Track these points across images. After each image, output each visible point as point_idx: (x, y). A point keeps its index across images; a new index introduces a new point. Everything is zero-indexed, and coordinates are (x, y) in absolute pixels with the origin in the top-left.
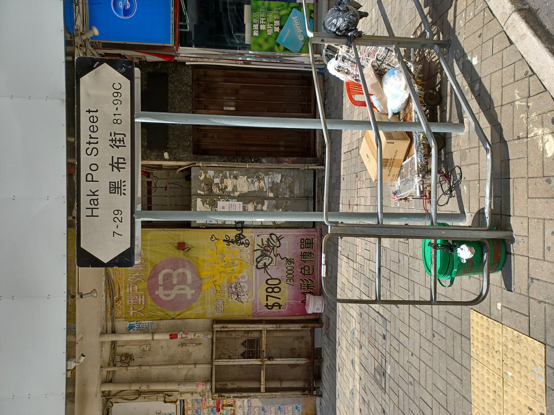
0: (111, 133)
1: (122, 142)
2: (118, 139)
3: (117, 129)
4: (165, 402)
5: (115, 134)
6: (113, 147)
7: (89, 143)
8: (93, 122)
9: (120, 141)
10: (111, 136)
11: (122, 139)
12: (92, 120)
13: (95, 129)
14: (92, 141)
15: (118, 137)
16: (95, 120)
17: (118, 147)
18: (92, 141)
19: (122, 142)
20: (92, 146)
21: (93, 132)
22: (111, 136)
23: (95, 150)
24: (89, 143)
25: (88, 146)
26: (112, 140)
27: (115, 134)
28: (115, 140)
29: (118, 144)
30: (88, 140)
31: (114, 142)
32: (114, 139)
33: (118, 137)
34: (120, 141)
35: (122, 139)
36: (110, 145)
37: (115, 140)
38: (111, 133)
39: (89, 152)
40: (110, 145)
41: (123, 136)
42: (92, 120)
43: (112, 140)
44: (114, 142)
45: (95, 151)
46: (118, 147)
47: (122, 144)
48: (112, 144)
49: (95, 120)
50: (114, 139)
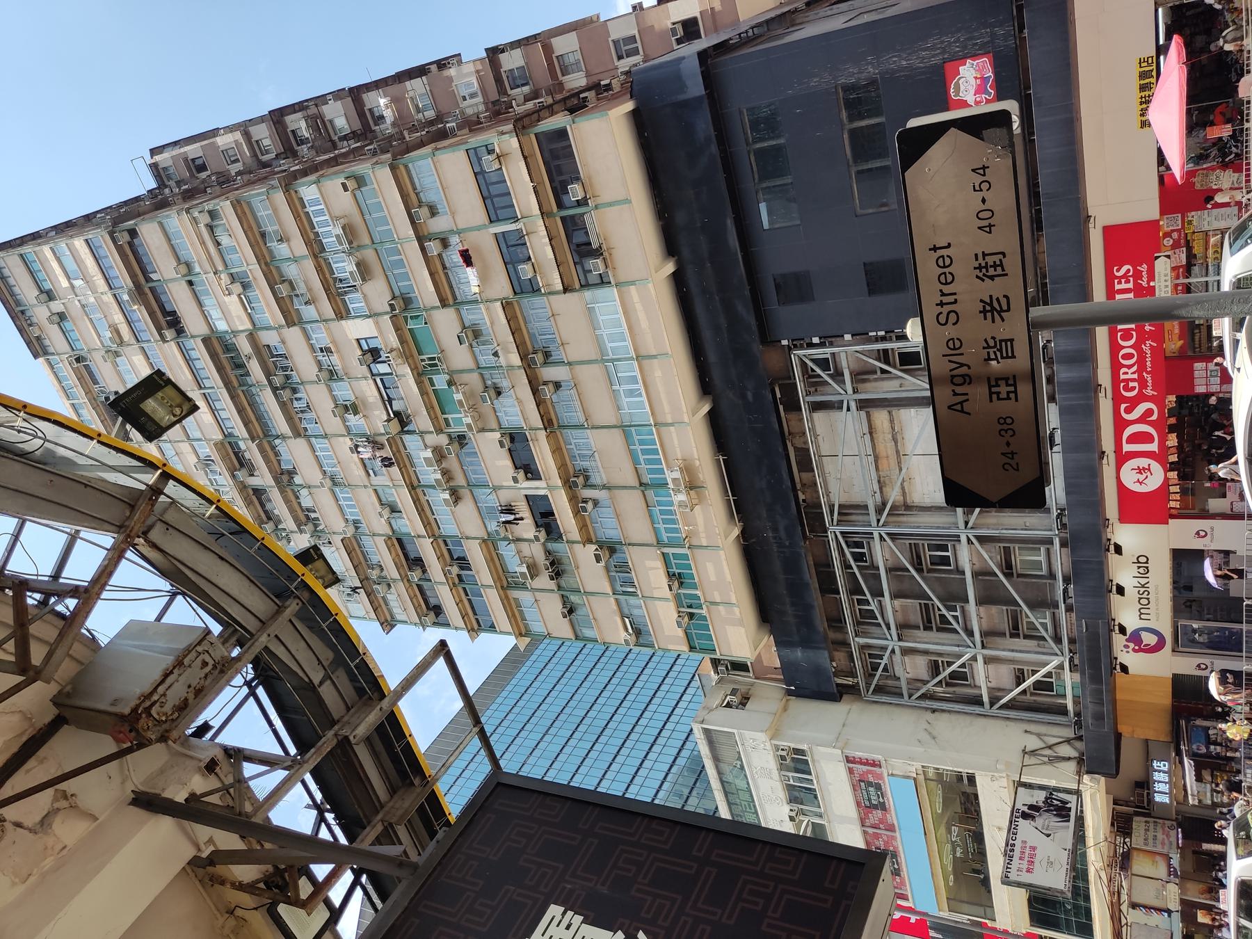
1: (999, 269)
3: (990, 243)
4: (1008, 310)
5: (984, 255)
7: (941, 304)
8: (944, 267)
12: (941, 263)
13: (950, 278)
14: (946, 299)
15: (990, 260)
16: (948, 261)
17: (992, 278)
18: (946, 299)
19: (999, 269)
20: (946, 309)
21: (946, 283)
23: (953, 316)
24: (941, 304)
25: (939, 309)
26: (980, 268)
27: (984, 255)
28: (986, 267)
29: (991, 272)
30: (938, 299)
33: (990, 260)
34: (995, 266)
37: (986, 267)
39: (942, 319)
41: (1001, 256)
42: (941, 263)
45: (953, 317)
48: (981, 275)
49: (948, 261)
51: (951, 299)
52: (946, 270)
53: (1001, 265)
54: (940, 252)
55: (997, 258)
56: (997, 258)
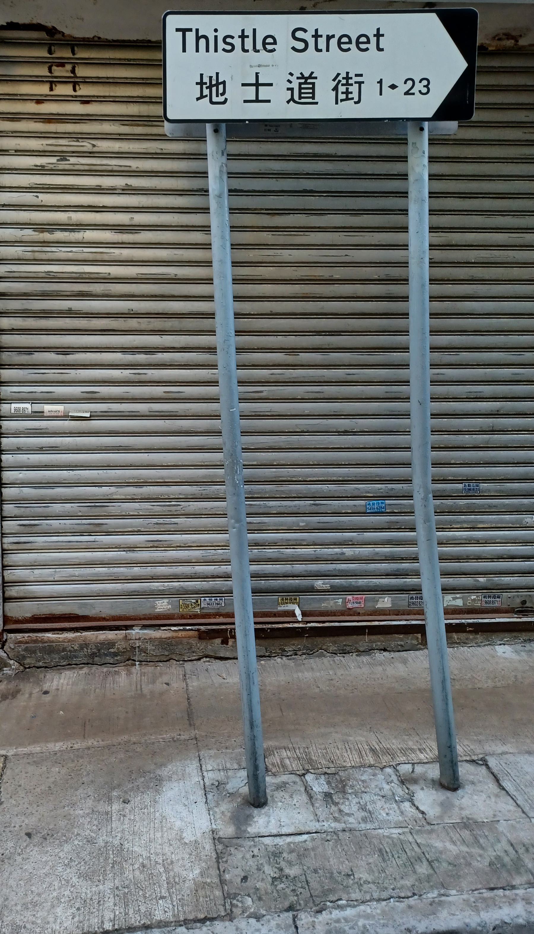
0: (361, 75)
1: (344, 96)
2: (351, 89)
5: (360, 83)
6: (334, 80)
9: (347, 93)
10: (356, 75)
11: (350, 96)
15: (354, 89)
17: (336, 89)
19: (344, 96)
22: (356, 75)
26: (347, 78)
27: (360, 83)
28: (347, 84)
29: (342, 89)
31: (344, 82)
32: (350, 81)
33: (354, 89)
34: (347, 93)
35: (350, 96)
36: (338, 75)
37: (347, 84)
38: (361, 75)
40: (338, 75)
41: (356, 99)
43: (347, 78)
44: (344, 82)
46: (336, 89)
47: (342, 96)
48: (340, 78)
50: (350, 81)
53: (347, 99)
54: (373, 40)
55: (355, 96)
56: (355, 96)
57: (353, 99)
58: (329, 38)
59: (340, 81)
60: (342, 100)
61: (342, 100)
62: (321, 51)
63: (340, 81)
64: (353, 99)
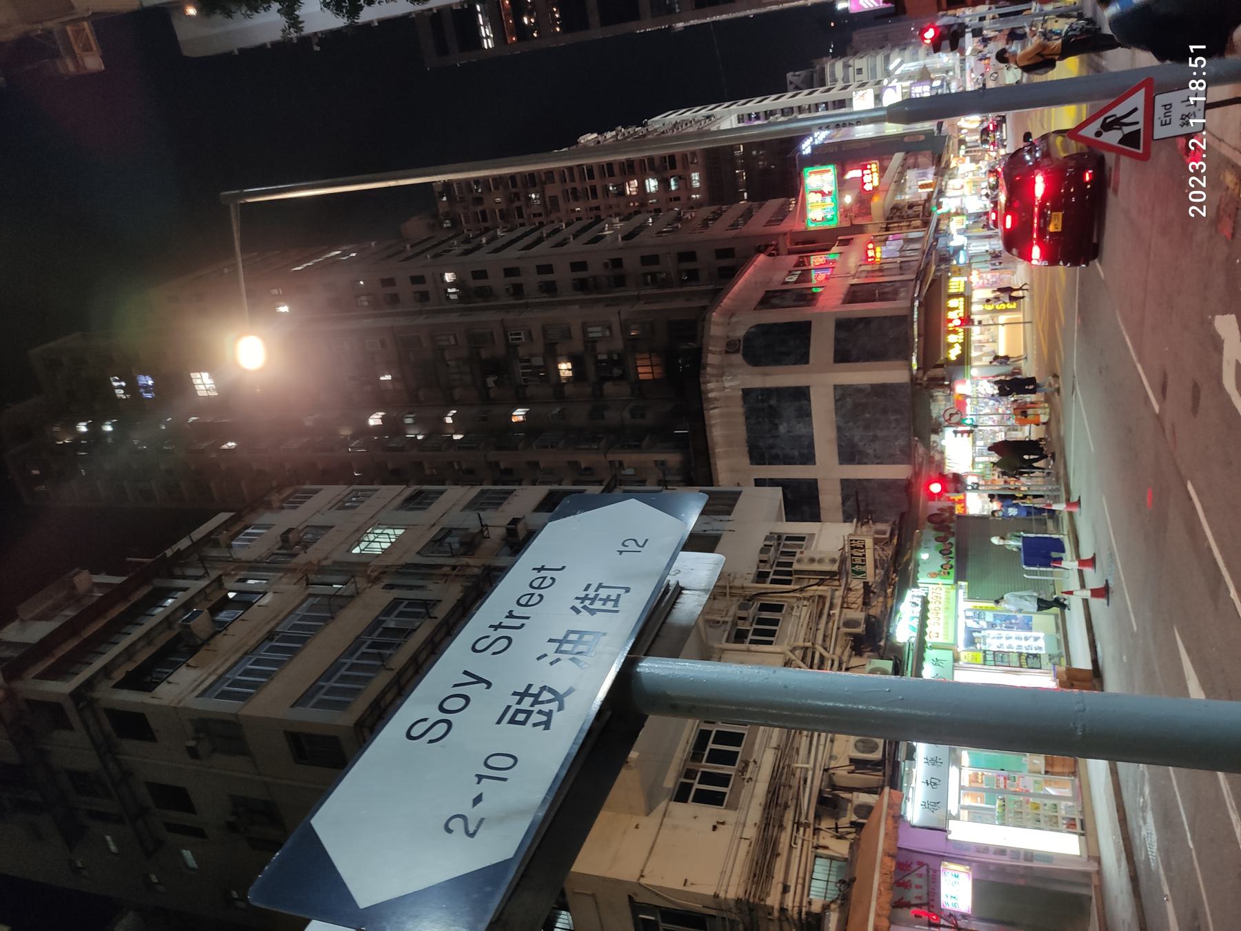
0: (589, 585)
15: (603, 593)
22: (586, 589)
34: (608, 599)
48: (579, 605)
51: (517, 623)
52: (538, 592)
53: (616, 601)
54: (543, 573)
55: (613, 594)
57: (619, 596)
58: (511, 615)
59: (584, 607)
60: (615, 606)
61: (615, 606)
62: (523, 625)
63: (584, 607)
64: (619, 596)
